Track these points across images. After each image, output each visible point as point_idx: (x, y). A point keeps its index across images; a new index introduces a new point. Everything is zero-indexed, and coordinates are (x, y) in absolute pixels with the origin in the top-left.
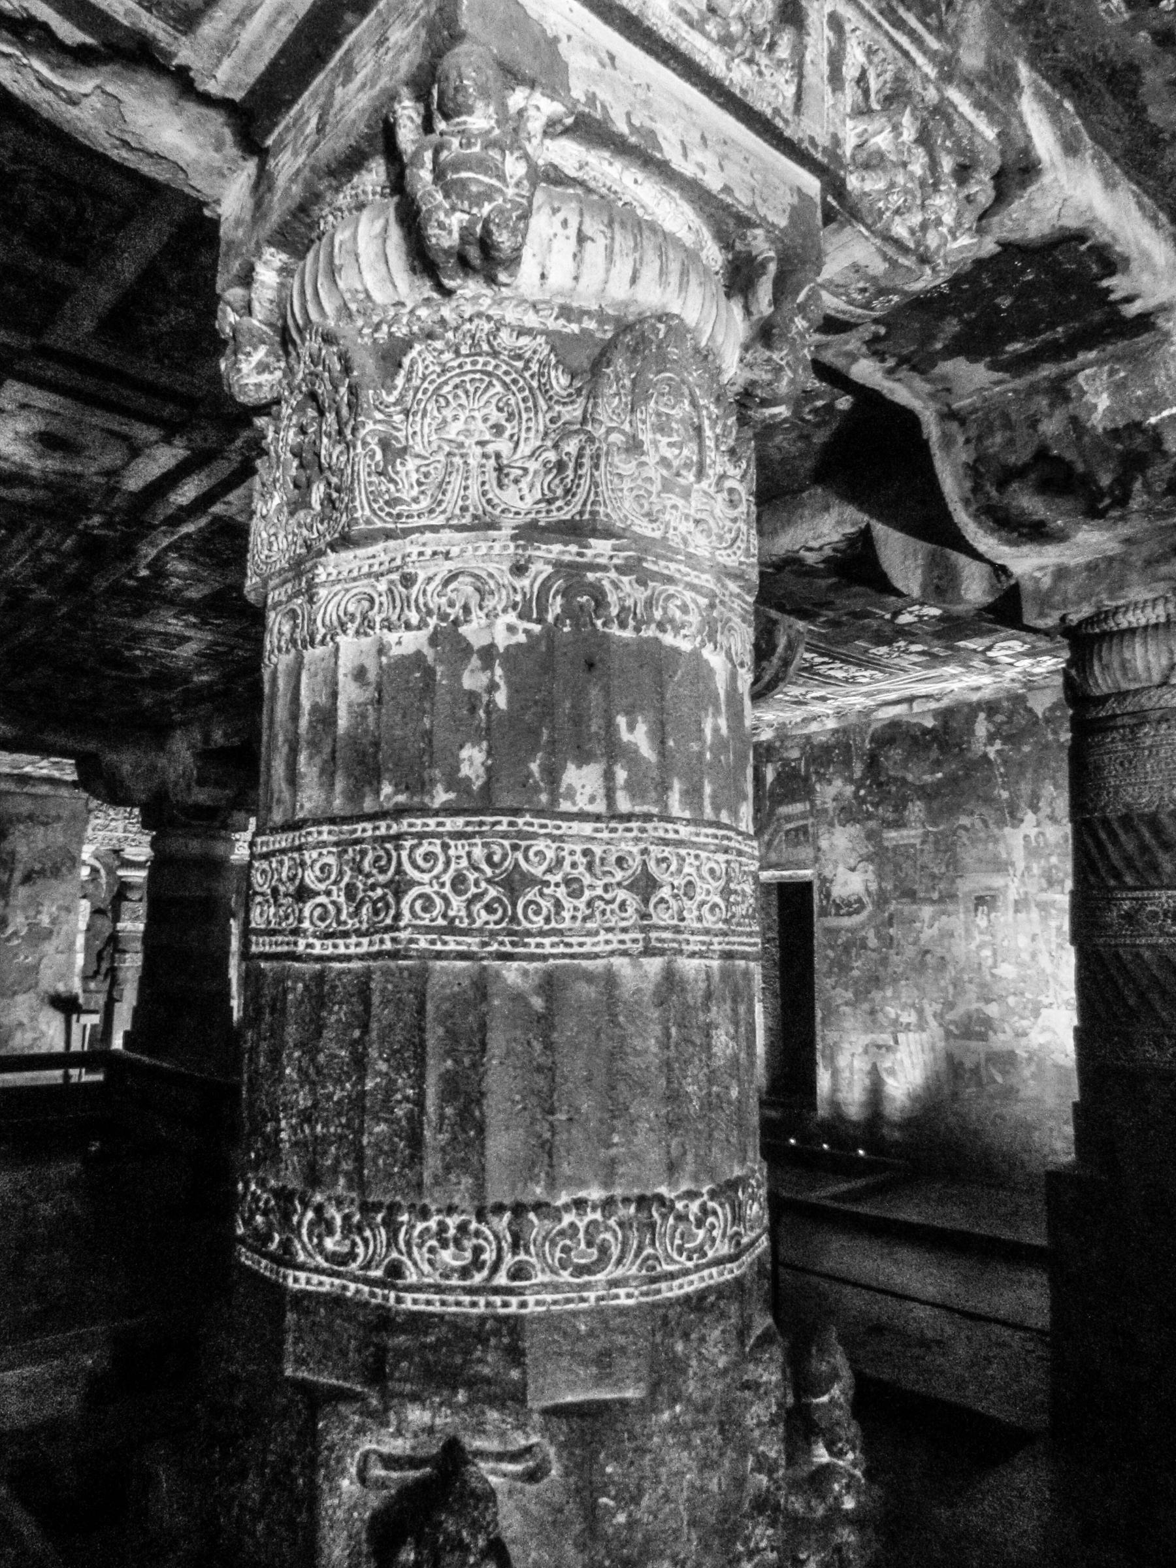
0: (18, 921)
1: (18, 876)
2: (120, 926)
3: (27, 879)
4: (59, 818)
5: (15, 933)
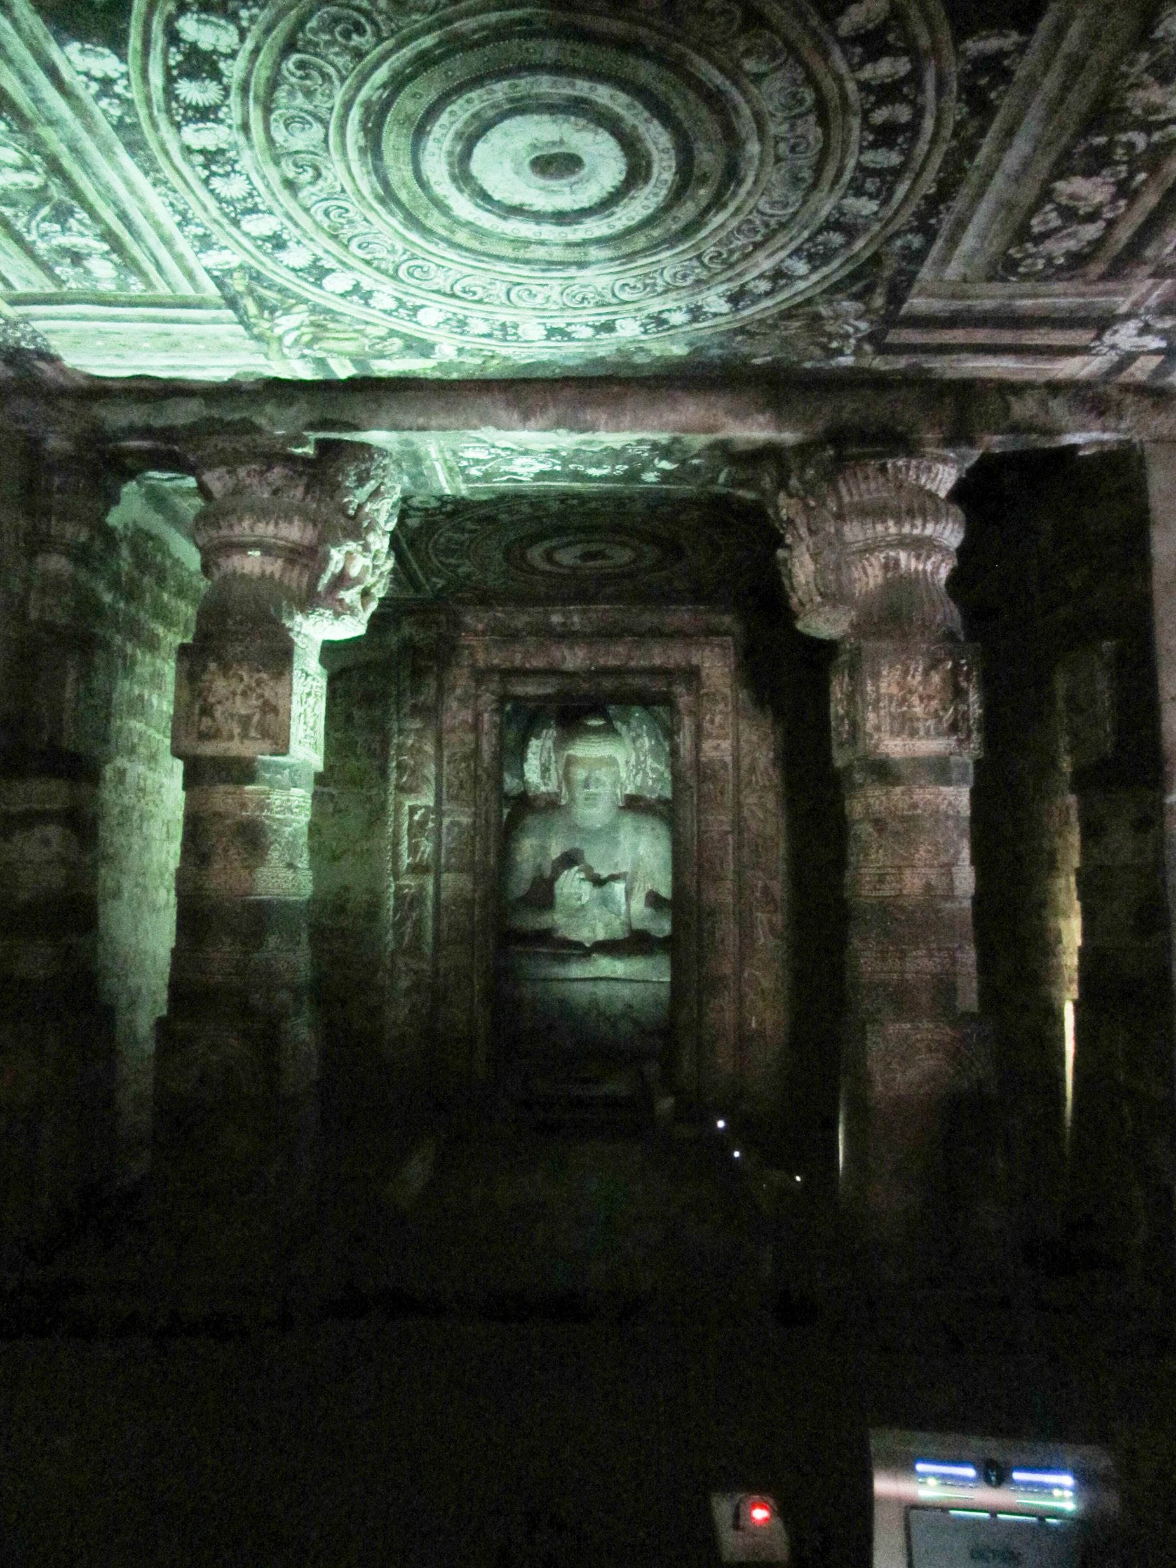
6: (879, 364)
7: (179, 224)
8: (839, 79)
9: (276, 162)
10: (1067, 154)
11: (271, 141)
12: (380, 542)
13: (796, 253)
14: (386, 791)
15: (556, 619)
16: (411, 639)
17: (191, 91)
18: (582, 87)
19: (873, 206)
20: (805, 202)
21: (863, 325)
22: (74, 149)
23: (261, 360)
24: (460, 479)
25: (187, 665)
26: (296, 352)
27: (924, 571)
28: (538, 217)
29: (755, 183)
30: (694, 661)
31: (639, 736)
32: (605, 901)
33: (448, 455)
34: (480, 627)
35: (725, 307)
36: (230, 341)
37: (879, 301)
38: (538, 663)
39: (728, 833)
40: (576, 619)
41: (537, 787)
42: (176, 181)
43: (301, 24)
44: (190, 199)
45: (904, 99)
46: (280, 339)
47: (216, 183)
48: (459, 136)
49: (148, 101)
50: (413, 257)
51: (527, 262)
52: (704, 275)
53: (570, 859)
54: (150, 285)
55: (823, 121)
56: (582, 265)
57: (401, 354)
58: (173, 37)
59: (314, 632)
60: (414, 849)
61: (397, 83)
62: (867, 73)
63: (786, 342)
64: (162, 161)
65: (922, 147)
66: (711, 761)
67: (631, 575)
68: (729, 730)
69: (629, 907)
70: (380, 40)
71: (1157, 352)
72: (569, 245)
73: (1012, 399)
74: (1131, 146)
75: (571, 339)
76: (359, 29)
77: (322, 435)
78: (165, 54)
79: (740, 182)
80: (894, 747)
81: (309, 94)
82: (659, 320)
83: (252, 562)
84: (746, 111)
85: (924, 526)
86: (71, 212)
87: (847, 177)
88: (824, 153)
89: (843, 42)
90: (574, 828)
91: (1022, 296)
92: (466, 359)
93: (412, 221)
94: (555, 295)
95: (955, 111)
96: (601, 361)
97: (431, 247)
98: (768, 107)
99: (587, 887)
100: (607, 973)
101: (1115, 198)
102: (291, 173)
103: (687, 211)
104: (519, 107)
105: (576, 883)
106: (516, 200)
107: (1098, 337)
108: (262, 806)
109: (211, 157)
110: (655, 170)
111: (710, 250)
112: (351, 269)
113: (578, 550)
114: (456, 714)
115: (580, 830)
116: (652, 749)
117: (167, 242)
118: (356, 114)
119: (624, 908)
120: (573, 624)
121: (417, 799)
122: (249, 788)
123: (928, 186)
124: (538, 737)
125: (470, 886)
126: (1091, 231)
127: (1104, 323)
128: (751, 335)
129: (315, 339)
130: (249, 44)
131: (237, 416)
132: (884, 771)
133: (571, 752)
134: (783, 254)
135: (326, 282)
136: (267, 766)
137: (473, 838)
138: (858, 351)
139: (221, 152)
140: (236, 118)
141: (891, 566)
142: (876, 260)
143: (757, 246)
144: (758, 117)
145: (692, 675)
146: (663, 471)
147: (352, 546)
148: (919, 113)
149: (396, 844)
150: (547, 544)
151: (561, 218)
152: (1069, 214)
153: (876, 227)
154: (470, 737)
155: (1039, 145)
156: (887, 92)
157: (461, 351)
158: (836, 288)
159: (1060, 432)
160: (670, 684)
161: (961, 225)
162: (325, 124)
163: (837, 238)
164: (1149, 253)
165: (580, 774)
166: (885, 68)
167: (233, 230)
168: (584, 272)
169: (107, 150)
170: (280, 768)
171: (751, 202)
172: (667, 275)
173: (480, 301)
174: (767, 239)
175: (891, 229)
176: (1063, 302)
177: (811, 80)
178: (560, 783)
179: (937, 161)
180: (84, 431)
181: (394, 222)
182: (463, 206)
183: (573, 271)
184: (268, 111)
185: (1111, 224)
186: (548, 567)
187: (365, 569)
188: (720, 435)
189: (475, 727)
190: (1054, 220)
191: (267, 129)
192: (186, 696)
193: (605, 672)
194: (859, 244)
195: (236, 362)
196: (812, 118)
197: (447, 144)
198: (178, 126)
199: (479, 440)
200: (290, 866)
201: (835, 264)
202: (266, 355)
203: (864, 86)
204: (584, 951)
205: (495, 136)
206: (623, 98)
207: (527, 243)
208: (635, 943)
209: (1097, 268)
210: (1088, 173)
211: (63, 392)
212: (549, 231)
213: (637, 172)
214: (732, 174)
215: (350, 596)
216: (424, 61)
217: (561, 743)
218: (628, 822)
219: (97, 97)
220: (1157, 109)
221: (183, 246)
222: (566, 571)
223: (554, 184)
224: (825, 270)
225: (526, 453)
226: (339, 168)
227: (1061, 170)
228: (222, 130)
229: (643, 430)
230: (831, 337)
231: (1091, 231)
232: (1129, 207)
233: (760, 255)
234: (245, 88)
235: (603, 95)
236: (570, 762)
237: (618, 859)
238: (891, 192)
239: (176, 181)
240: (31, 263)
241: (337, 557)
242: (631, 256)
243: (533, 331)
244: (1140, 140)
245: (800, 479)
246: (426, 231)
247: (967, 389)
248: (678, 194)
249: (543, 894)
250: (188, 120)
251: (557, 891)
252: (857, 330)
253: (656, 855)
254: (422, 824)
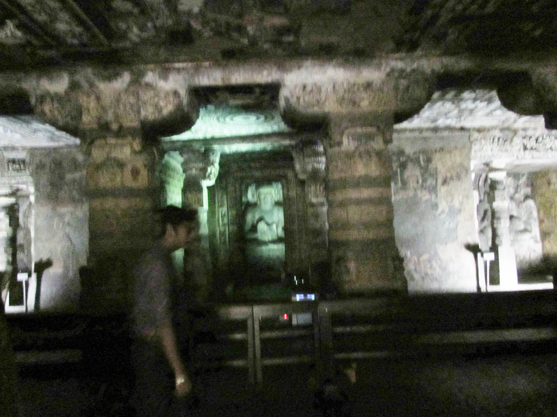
0: (443, 205)
1: (440, 181)
2: (495, 204)
3: (445, 182)
4: (456, 148)
5: (443, 212)
12: (217, 165)
32: (271, 230)
53: (261, 219)
59: (206, 184)
60: (223, 221)
69: (278, 230)
80: (314, 200)
83: (194, 171)
90: (262, 211)
132: (312, 205)
141: (313, 166)
149: (218, 221)
165: (262, 197)
204: (265, 243)
208: (279, 240)
217: (257, 188)
241: (209, 169)
249: (254, 228)
254: (224, 215)
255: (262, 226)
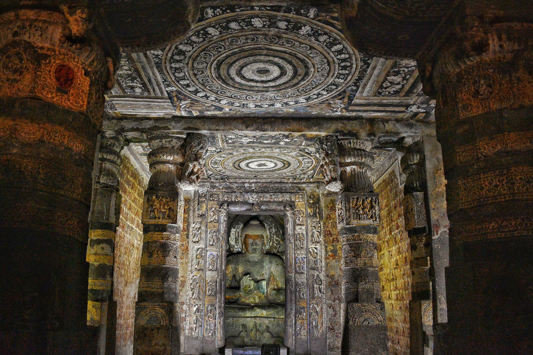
6: (347, 114)
7: (163, 82)
8: (333, 58)
9: (193, 70)
10: (389, 72)
11: (193, 66)
13: (324, 89)
14: (188, 242)
15: (246, 185)
16: (198, 191)
17: (177, 57)
18: (271, 58)
19: (343, 81)
20: (325, 79)
21: (342, 105)
22: (143, 68)
23: (174, 111)
24: (225, 143)
25: (146, 198)
26: (184, 109)
27: (362, 172)
28: (257, 82)
29: (313, 76)
30: (293, 200)
31: (271, 228)
32: (259, 288)
33: (223, 137)
34: (221, 187)
35: (305, 101)
36: (166, 106)
37: (346, 100)
38: (240, 199)
39: (304, 258)
40: (253, 185)
41: (234, 246)
42: (166, 73)
43: (207, 47)
44: (168, 77)
45: (348, 61)
46: (181, 106)
47: (176, 74)
48: (240, 66)
49: (166, 59)
50: (223, 89)
51: (252, 91)
52: (299, 94)
54: (150, 94)
55: (329, 65)
56: (268, 91)
57: (214, 110)
58: (176, 48)
61: (227, 57)
62: (339, 57)
63: (322, 109)
64: (164, 70)
65: (353, 70)
66: (299, 234)
67: (273, 171)
68: (305, 223)
70: (225, 50)
71: (424, 112)
72: (264, 87)
73: (385, 124)
74: (404, 71)
75: (262, 107)
76: (221, 48)
77: (188, 131)
78: (173, 51)
79: (309, 76)
81: (205, 58)
82: (286, 104)
84: (310, 63)
85: (362, 159)
86: (136, 79)
87: (335, 75)
88: (330, 71)
89: (333, 52)
91: (384, 100)
92: (231, 112)
93: (224, 82)
94: (259, 98)
95: (360, 64)
96: (270, 113)
97: (228, 88)
98: (315, 62)
99: (252, 283)
100: (260, 315)
101: (403, 80)
102: (196, 72)
103: (295, 81)
104: (255, 62)
105: (248, 281)
106: (252, 78)
107: (407, 109)
108: (168, 239)
109: (176, 69)
110: (288, 73)
111: (301, 89)
112: (205, 91)
113: (256, 163)
114: (211, 217)
115: (249, 261)
116: (276, 232)
117: (158, 85)
118: (215, 62)
119: (266, 291)
120: (252, 187)
121: (199, 245)
122: (164, 233)
123: (356, 77)
124: (234, 228)
125: (217, 276)
126: (399, 87)
127: (407, 106)
128: (312, 107)
129: (191, 106)
130: (194, 50)
131: (164, 126)
133: (247, 233)
134: (320, 90)
135: (197, 94)
136: (170, 227)
137: (217, 259)
138: (341, 111)
139: (180, 68)
140: (186, 62)
142: (344, 91)
143: (313, 88)
144: (313, 64)
145: (292, 205)
146: (286, 142)
147: (195, 163)
148: (352, 64)
150: (247, 161)
151: (262, 82)
152: (392, 83)
153: (344, 85)
154: (216, 224)
155: (381, 70)
156: (344, 60)
157: (230, 110)
158: (335, 97)
159: (399, 133)
160: (285, 207)
161: (365, 85)
162: (207, 64)
163: (334, 87)
164: (415, 91)
165: (250, 241)
166: (343, 56)
167: (177, 83)
168: (268, 93)
169: (151, 68)
170: (173, 227)
171: (312, 79)
172: (289, 94)
173: (239, 99)
174: (316, 87)
175: (348, 85)
176: (395, 101)
177: (325, 57)
178: (242, 245)
179: (357, 73)
180: (119, 129)
181: (219, 82)
182: (238, 79)
183: (264, 93)
184: (194, 60)
185: (403, 85)
186: (246, 168)
187: (198, 169)
188: (303, 133)
189: (218, 221)
190: (389, 84)
191: (193, 63)
192: (146, 206)
193: (263, 203)
194: (340, 88)
195: (166, 111)
196: (326, 64)
197: (236, 68)
198: (171, 63)
199: (233, 133)
200: (175, 257)
201: (334, 92)
202: (175, 110)
203: (338, 59)
204: (251, 307)
205: (249, 67)
206: (281, 60)
207: (253, 87)
209: (403, 94)
210: (395, 76)
211: (113, 118)
212: (258, 85)
213: (283, 73)
214: (307, 74)
215: (194, 177)
216: (234, 54)
218: (267, 259)
219: (154, 58)
220: (408, 64)
221: (162, 86)
222: (251, 170)
223: (262, 75)
224: (331, 94)
225: (246, 136)
226: (208, 72)
227: (388, 75)
228: (182, 64)
229: (281, 131)
230: (334, 108)
231: (399, 87)
232: (407, 82)
233: (314, 90)
234: (190, 57)
235: (276, 60)
236: (247, 236)
237: (264, 272)
238: (347, 79)
239: (166, 73)
240: (120, 89)
241: (191, 166)
242: (280, 90)
243: (252, 106)
244: (406, 70)
245: (326, 145)
246: (227, 84)
247: (372, 121)
248: (293, 78)
250: (174, 62)
251: (241, 284)
252: (341, 106)
253: (278, 271)
255: (247, 281)
